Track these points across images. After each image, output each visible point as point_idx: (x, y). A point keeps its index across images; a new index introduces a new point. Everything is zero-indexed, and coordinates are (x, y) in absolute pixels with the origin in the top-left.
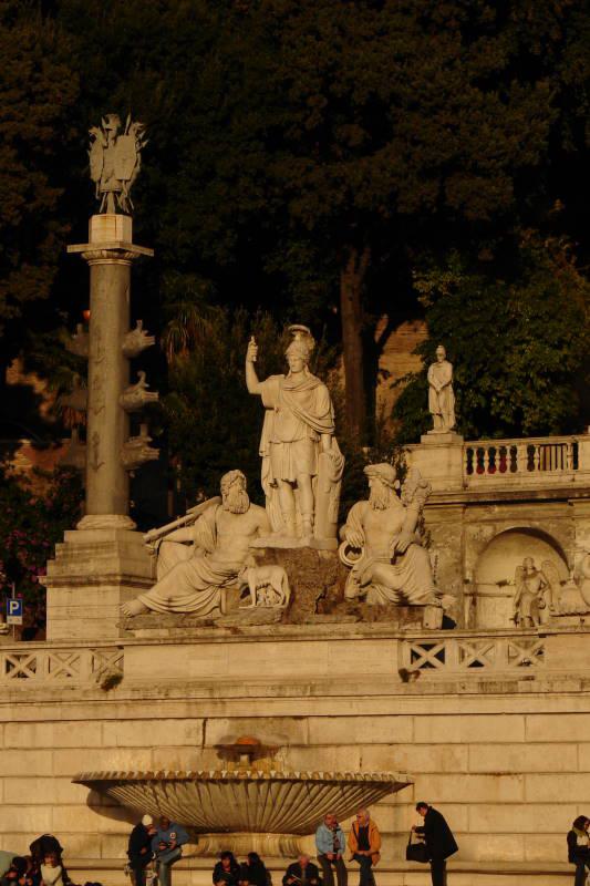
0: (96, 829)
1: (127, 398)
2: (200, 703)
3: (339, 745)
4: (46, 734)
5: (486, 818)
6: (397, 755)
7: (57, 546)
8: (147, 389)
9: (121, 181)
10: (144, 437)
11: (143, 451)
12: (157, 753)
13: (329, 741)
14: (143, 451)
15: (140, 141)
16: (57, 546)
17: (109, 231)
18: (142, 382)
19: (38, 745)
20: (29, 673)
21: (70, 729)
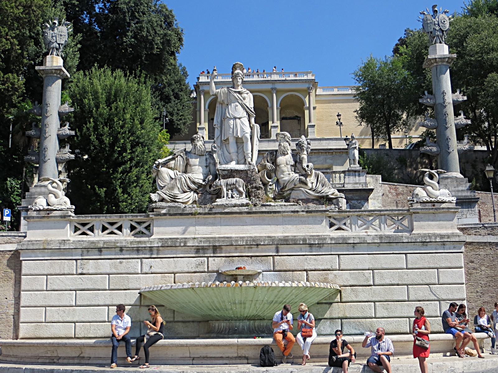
0: (138, 319)
1: (60, 132)
2: (206, 249)
3: (293, 271)
4: (106, 266)
5: (387, 309)
6: (331, 275)
7: (27, 193)
8: (69, 129)
9: (59, 44)
10: (67, 149)
11: (67, 154)
12: (176, 275)
13: (288, 268)
14: (67, 154)
15: (68, 30)
16: (27, 193)
17: (55, 61)
18: (67, 127)
19: (99, 271)
20: (89, 232)
21: (121, 263)
